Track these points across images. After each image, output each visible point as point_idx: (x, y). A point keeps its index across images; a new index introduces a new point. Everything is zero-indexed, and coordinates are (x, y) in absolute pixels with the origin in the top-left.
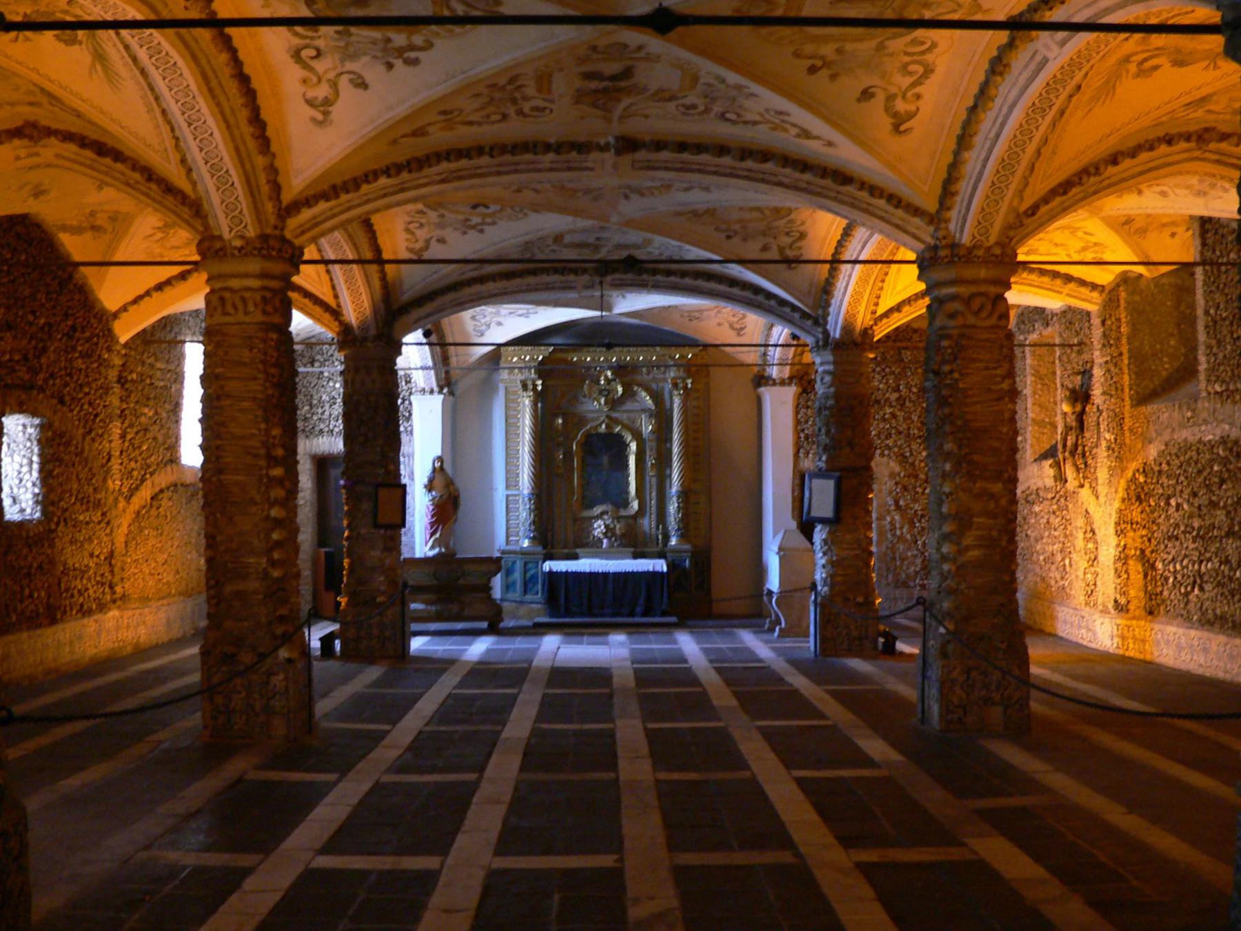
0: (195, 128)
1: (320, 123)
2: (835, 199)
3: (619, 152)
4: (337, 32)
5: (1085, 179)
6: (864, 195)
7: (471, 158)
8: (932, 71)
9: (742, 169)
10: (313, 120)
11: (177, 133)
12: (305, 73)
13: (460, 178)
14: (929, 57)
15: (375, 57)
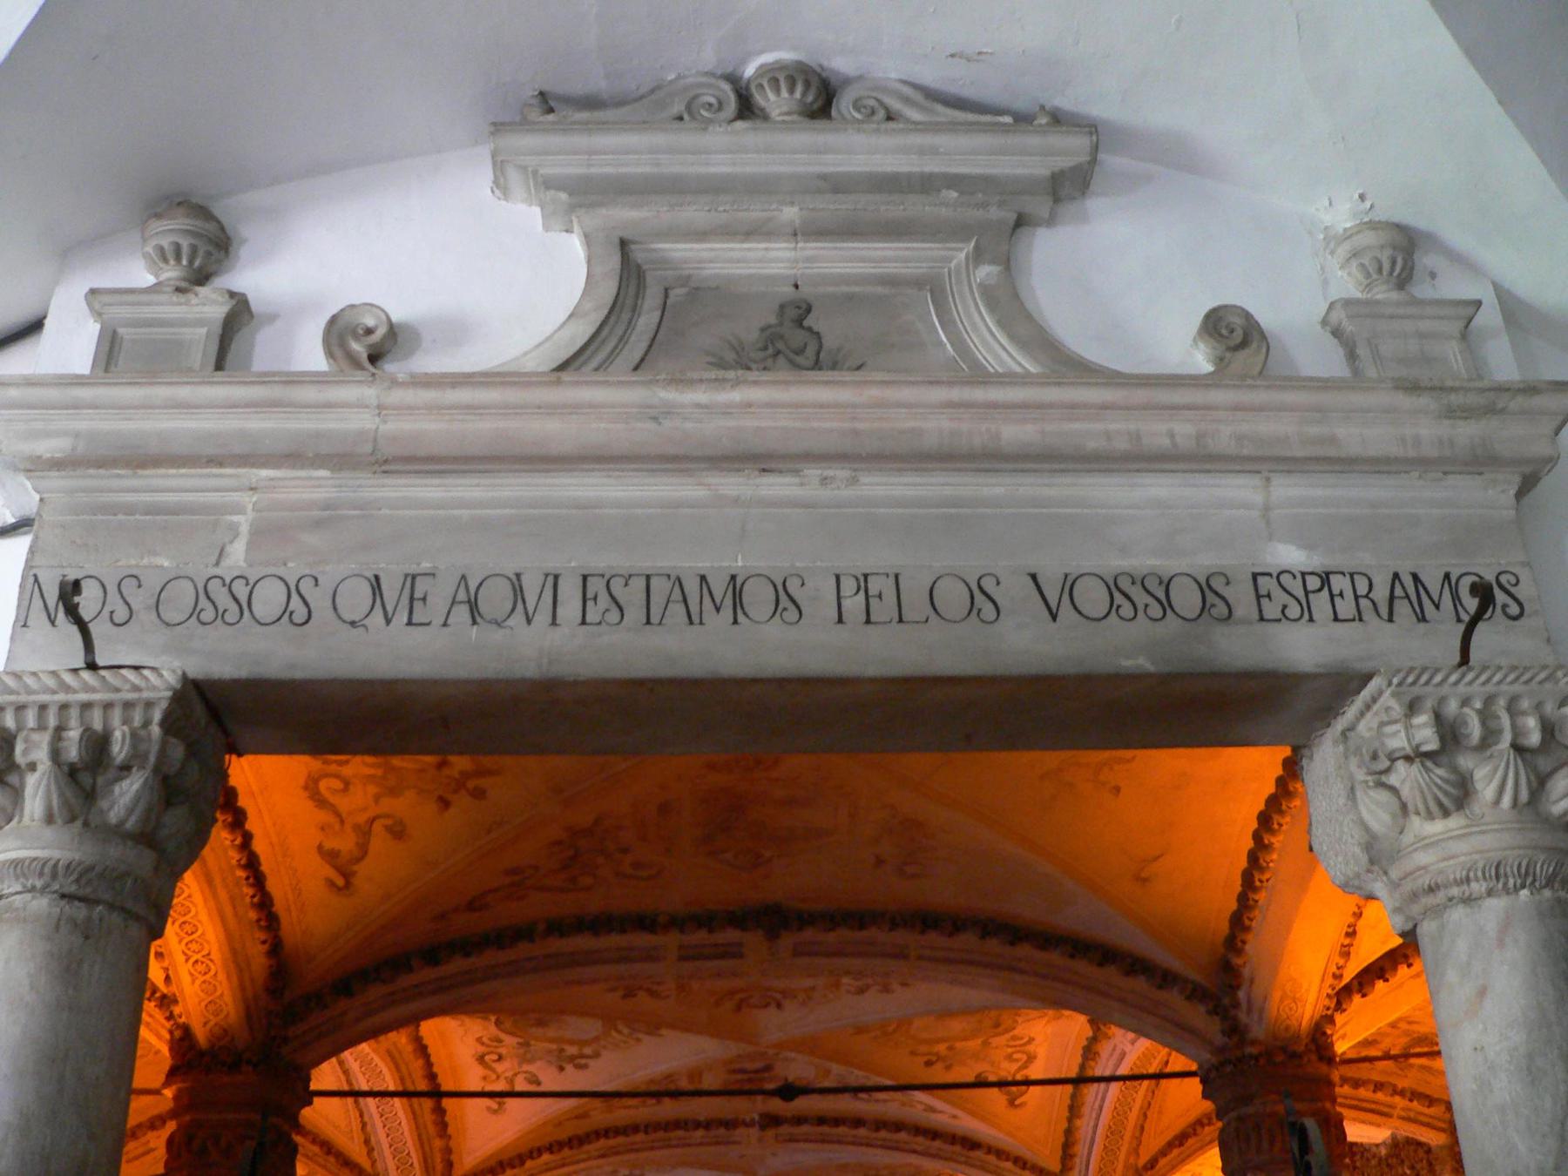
0: (386, 1119)
1: (495, 1112)
2: (966, 1163)
3: (763, 1127)
4: (518, 1043)
5: (1199, 1129)
6: (992, 1159)
7: (627, 1136)
8: (1035, 1057)
9: (876, 1139)
10: (489, 1108)
11: (366, 1119)
12: (489, 1073)
13: (617, 1153)
14: (1031, 1048)
15: (549, 1061)
